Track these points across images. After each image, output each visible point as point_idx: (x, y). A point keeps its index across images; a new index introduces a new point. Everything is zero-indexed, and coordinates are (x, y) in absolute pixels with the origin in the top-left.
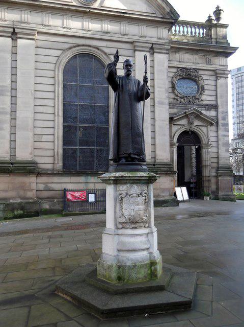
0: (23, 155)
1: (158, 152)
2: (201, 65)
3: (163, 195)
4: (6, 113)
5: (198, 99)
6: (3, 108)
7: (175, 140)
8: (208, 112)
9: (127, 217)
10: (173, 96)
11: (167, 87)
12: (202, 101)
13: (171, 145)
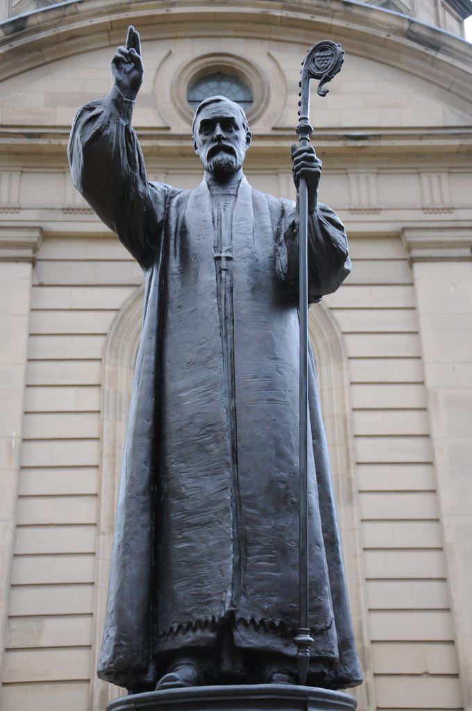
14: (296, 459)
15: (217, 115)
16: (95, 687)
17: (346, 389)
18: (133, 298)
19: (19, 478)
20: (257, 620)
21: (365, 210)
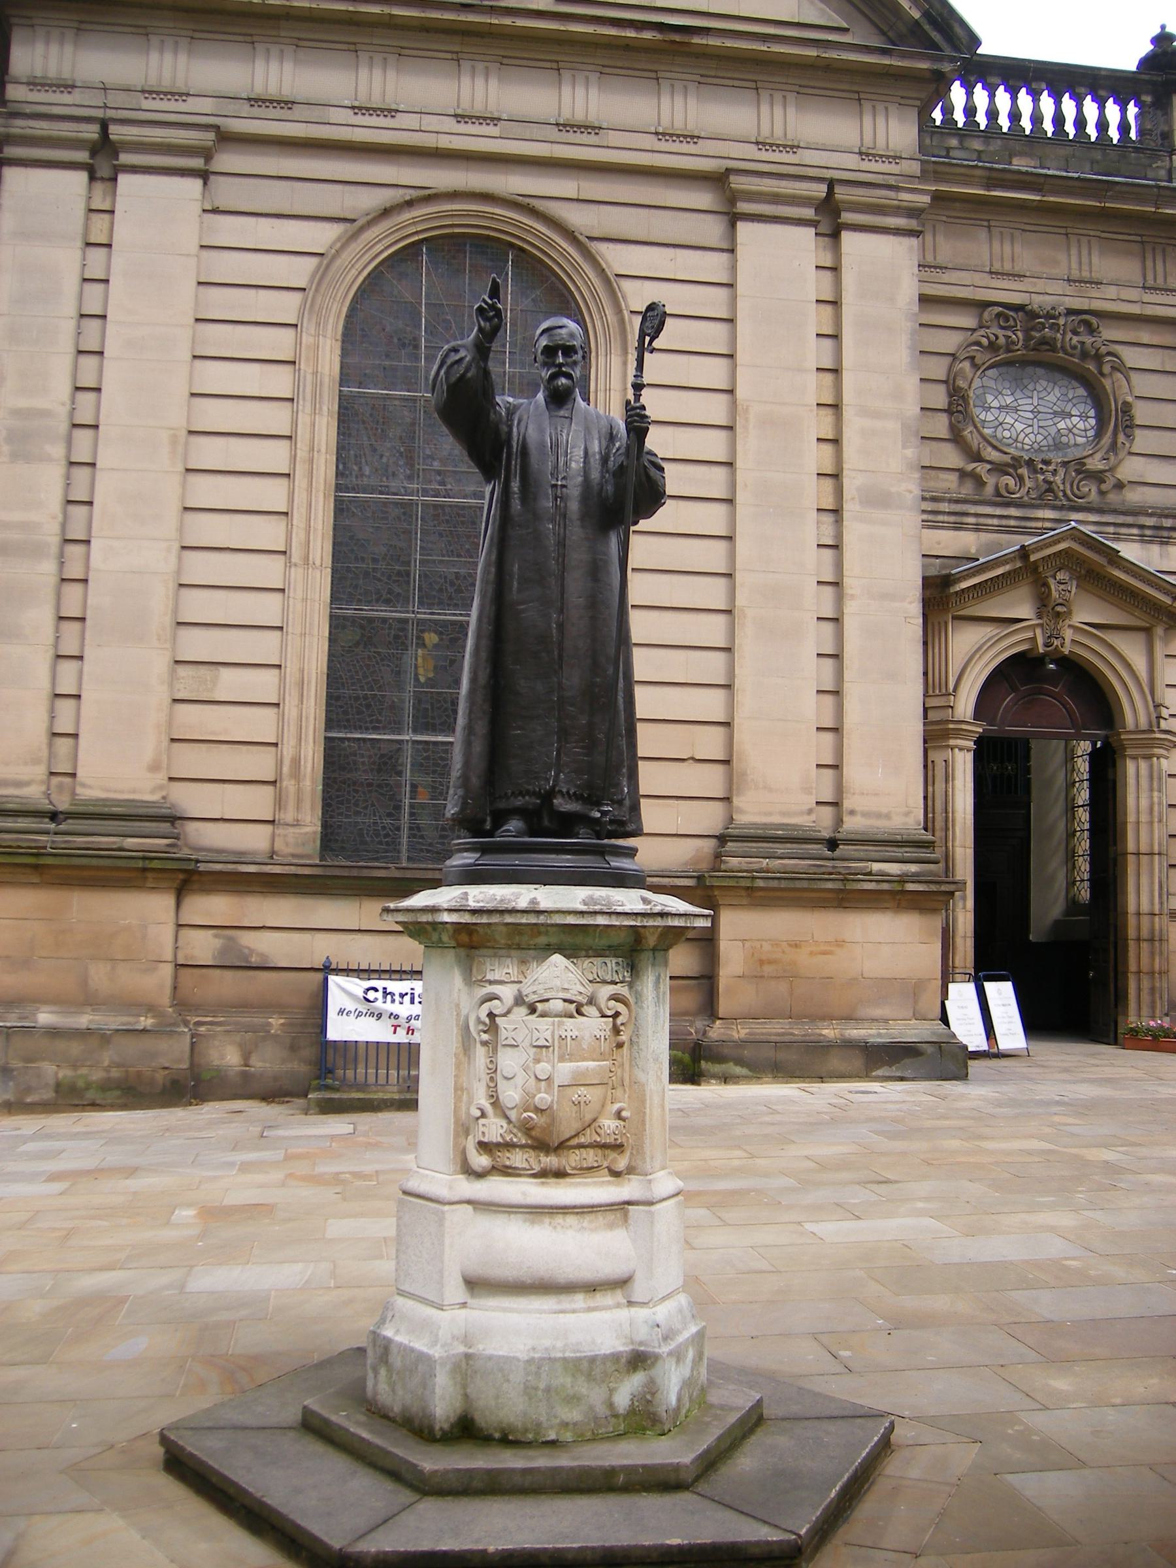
0: (116, 770)
1: (853, 772)
2: (1112, 292)
3: (878, 1012)
4: (35, 551)
5: (1097, 477)
6: (25, 526)
7: (965, 704)
8: (1155, 549)
9: (513, 1115)
10: (951, 457)
11: (912, 409)
12: (1120, 486)
13: (936, 735)
14: (611, 671)
16: (285, 753)
18: (344, 240)
19: (184, 485)
21: (678, 136)
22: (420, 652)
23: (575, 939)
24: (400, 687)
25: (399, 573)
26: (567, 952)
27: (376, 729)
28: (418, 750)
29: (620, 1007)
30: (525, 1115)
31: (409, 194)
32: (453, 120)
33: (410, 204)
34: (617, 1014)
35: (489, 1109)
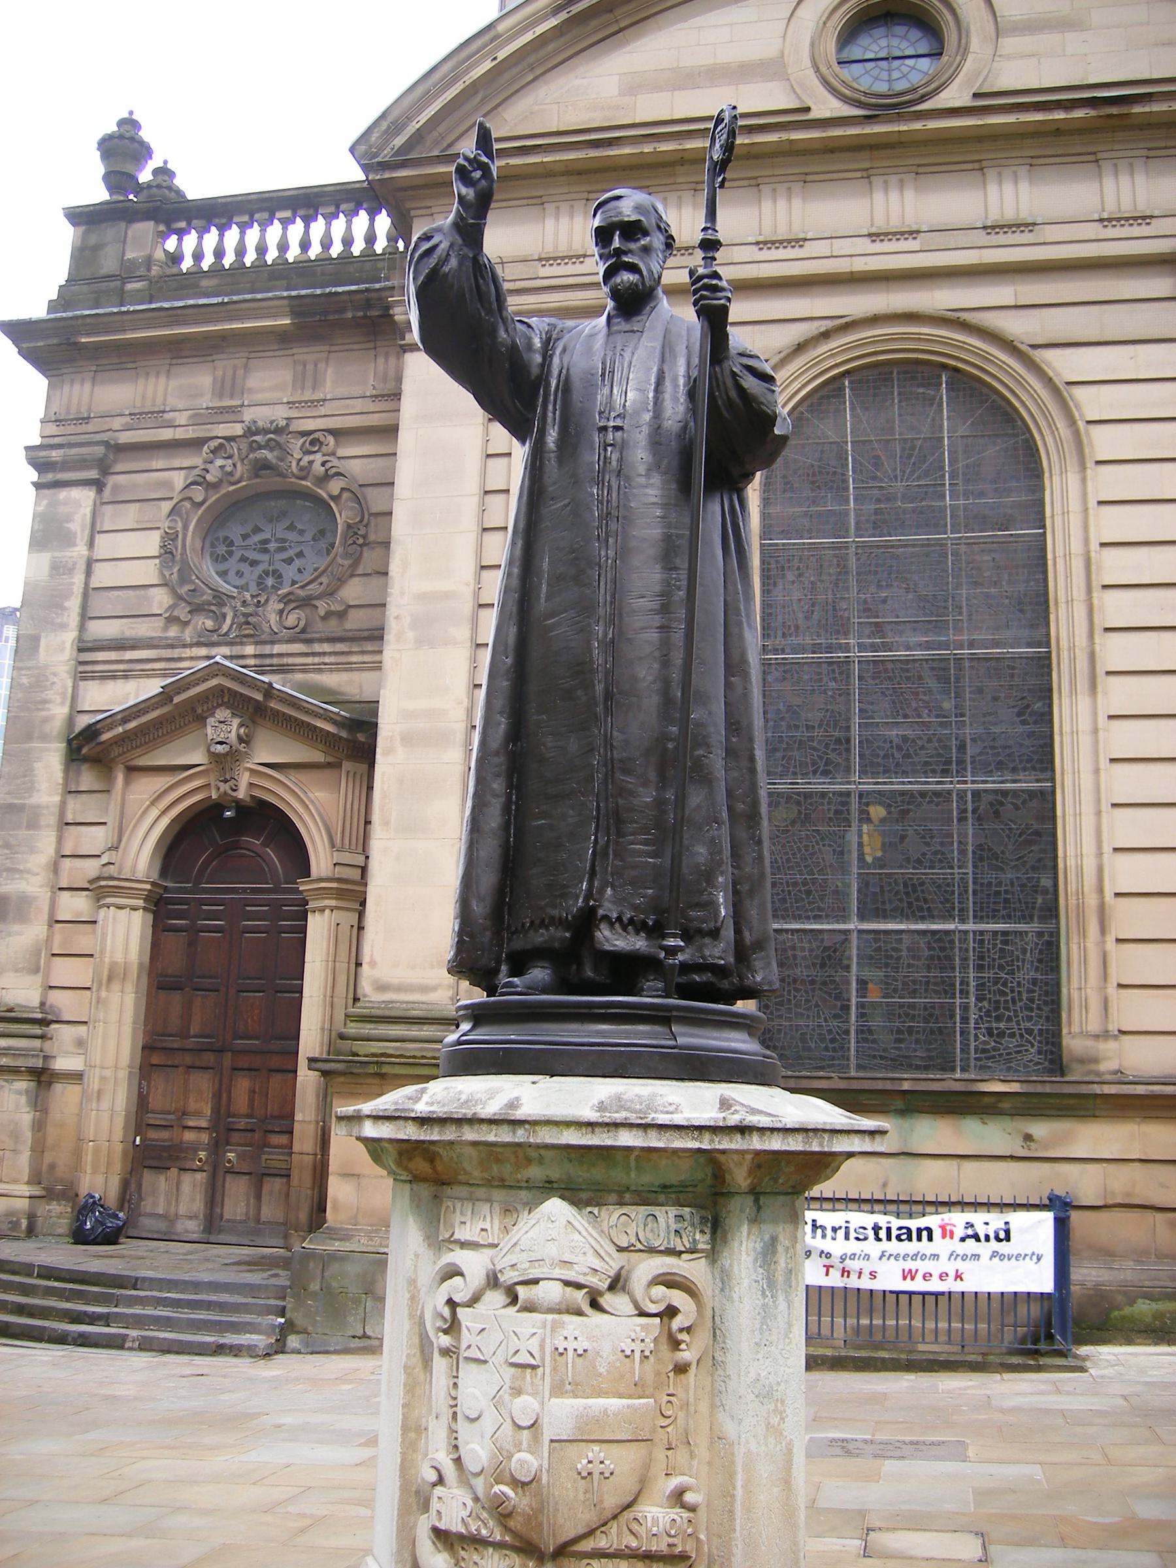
9: (479, 1484)
15: (614, 219)
17: (1091, 511)
20: (628, 915)
21: (1127, 219)
22: (865, 827)
23: (591, 1174)
24: (844, 869)
25: (838, 741)
26: (584, 1196)
27: (817, 918)
28: (867, 941)
29: (678, 1298)
30: (497, 1488)
31: (824, 326)
32: (867, 241)
33: (826, 335)
34: (671, 1312)
35: (449, 1471)
